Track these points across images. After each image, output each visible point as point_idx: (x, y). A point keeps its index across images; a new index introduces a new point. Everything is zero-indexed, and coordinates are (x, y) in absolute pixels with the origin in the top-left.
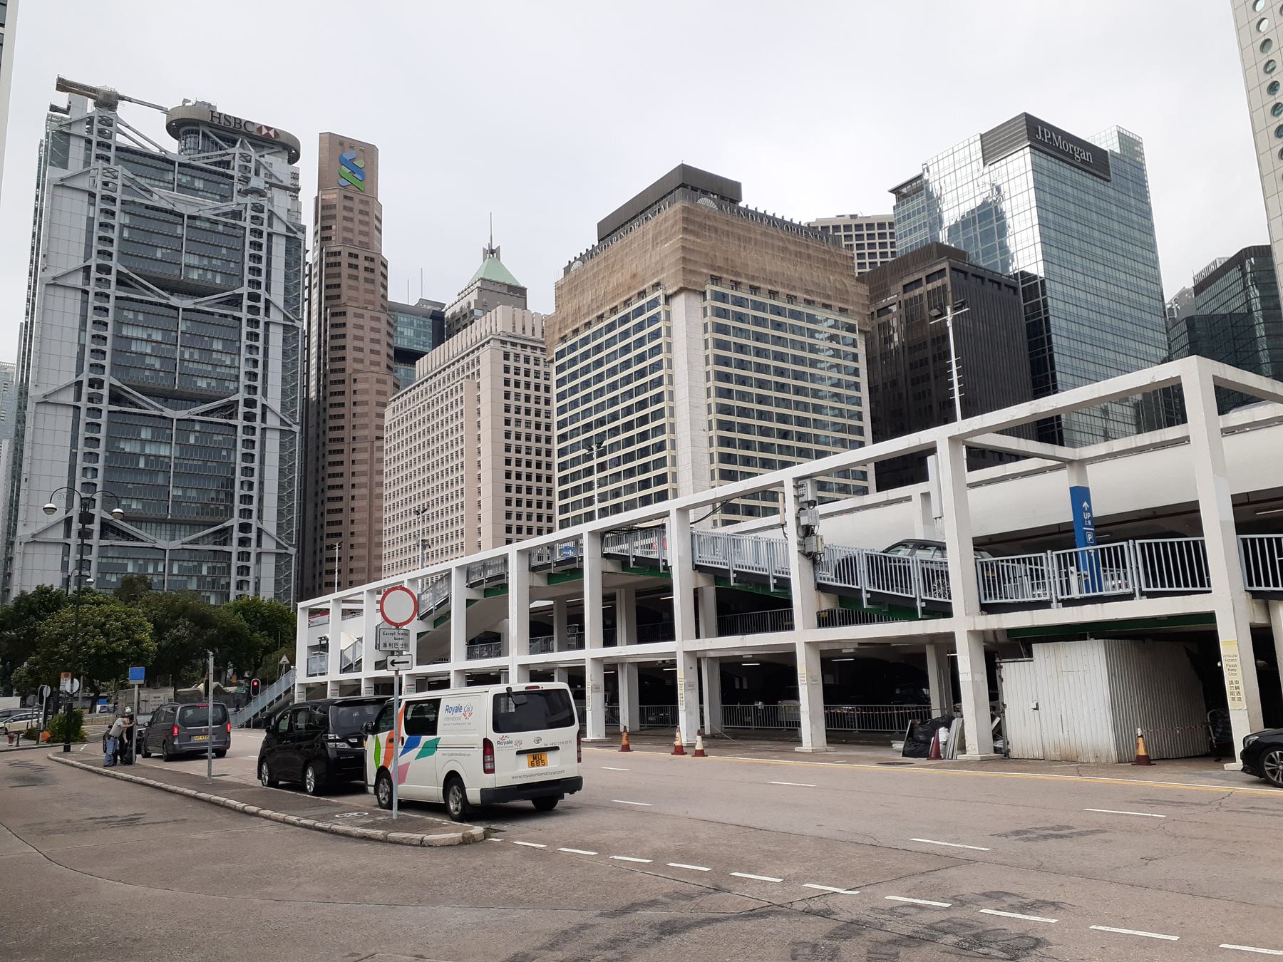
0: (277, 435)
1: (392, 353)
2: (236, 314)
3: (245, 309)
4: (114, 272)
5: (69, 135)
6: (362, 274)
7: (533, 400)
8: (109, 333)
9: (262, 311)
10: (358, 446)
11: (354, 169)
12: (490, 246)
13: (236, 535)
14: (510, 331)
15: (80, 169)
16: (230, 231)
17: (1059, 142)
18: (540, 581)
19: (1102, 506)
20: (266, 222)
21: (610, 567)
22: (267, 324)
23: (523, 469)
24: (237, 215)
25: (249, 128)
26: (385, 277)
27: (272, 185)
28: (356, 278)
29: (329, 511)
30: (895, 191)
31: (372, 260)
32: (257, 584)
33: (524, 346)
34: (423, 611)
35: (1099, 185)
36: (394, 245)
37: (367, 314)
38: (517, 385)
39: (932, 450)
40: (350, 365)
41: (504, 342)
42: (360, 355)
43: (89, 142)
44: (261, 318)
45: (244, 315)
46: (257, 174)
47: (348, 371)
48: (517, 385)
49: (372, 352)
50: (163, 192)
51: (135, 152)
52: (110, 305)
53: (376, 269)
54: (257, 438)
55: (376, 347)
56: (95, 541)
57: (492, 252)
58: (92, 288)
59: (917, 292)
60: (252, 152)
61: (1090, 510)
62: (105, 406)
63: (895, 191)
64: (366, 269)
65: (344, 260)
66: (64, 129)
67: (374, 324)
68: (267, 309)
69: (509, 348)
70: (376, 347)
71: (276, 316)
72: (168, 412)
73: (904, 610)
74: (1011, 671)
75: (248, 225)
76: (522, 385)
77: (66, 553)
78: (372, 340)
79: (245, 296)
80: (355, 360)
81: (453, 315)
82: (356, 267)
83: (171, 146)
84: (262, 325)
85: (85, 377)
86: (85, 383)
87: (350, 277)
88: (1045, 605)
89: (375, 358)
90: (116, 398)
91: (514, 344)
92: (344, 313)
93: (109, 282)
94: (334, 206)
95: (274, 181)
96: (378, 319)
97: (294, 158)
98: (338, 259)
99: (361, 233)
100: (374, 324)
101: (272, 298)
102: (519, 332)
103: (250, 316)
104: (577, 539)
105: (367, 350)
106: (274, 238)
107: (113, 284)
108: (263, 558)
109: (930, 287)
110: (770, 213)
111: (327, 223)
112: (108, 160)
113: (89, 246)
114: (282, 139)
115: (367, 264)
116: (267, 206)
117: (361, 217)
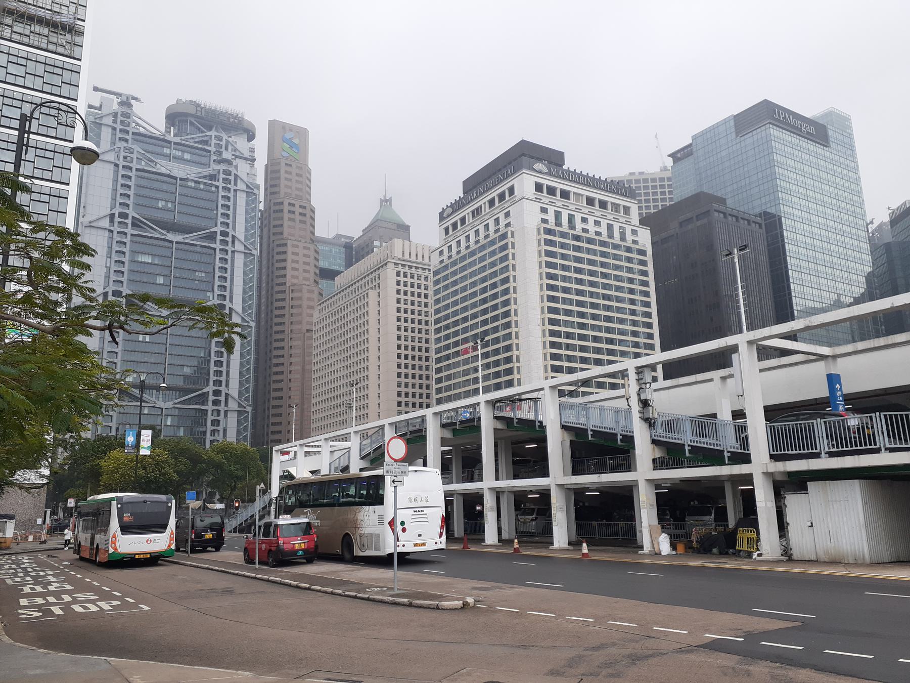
1: (318, 272)
2: (212, 245)
3: (218, 242)
4: (130, 217)
5: (101, 124)
6: (298, 217)
7: (416, 304)
8: (126, 259)
9: (230, 244)
10: (293, 336)
11: (292, 146)
12: (385, 197)
13: (211, 398)
14: (400, 256)
15: (108, 148)
16: (208, 188)
17: (791, 120)
18: (448, 434)
19: (850, 386)
20: (232, 182)
21: (499, 426)
22: (233, 252)
23: (410, 353)
24: (213, 177)
26: (314, 219)
27: (236, 157)
28: (293, 220)
29: (274, 382)
30: (672, 155)
31: (305, 208)
32: (225, 430)
33: (410, 267)
34: (364, 453)
35: (820, 150)
36: (320, 197)
37: (301, 245)
38: (405, 293)
39: (734, 349)
40: (290, 280)
41: (396, 264)
42: (296, 273)
43: (114, 129)
44: (229, 248)
45: (218, 246)
46: (226, 149)
47: (288, 285)
48: (405, 293)
49: (305, 271)
50: (163, 162)
51: (145, 136)
52: (128, 240)
53: (307, 215)
55: (307, 268)
57: (386, 201)
58: (116, 228)
59: (690, 227)
61: (841, 390)
63: (672, 155)
64: (301, 214)
65: (286, 208)
66: (98, 121)
67: (306, 252)
68: (233, 242)
69: (400, 268)
70: (307, 268)
71: (239, 247)
73: (714, 457)
74: (793, 501)
75: (221, 184)
76: (409, 294)
78: (305, 263)
79: (219, 233)
80: (293, 277)
81: (359, 246)
82: (294, 212)
84: (230, 253)
86: (110, 293)
87: (290, 219)
88: (817, 456)
89: (306, 275)
91: (403, 265)
92: (285, 245)
93: (126, 224)
94: (279, 171)
95: (237, 154)
96: (308, 249)
97: (251, 137)
98: (281, 207)
99: (297, 189)
100: (306, 252)
101: (237, 235)
102: (407, 257)
103: (221, 247)
104: (475, 406)
105: (301, 270)
106: (238, 192)
107: (130, 226)
108: (229, 414)
109: (699, 223)
110: (584, 173)
111: (273, 183)
112: (127, 141)
113: (114, 199)
114: (245, 126)
115: (301, 210)
116: (234, 171)
117: (297, 178)
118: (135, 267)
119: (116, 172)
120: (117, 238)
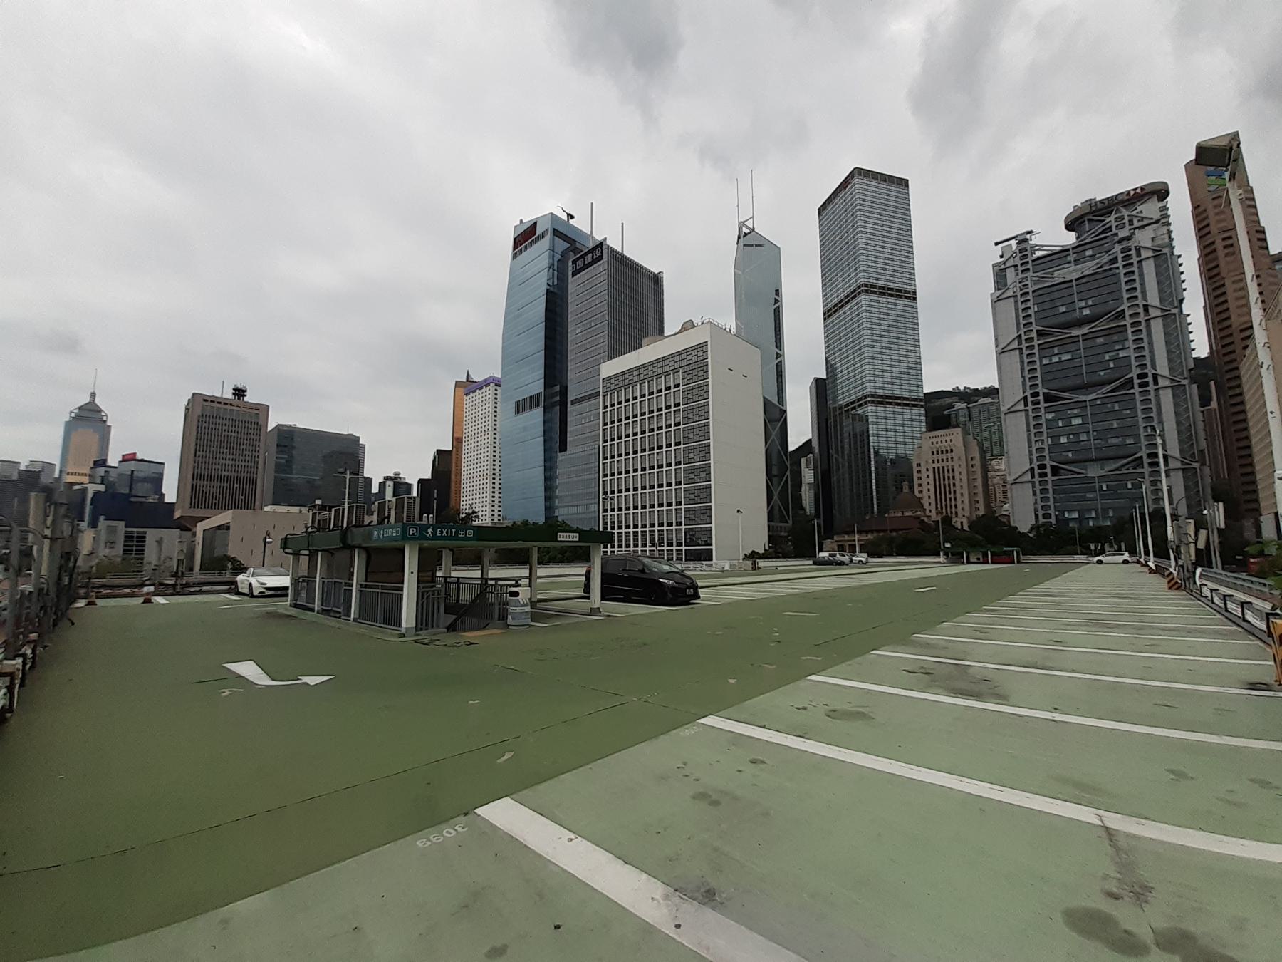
0: (1170, 390)
13: (1146, 461)
25: (1120, 198)
44: (1142, 318)
46: (1131, 222)
54: (1152, 396)
56: (1050, 478)
58: (1024, 345)
60: (1125, 213)
62: (1042, 405)
71: (1153, 313)
72: (1082, 398)
75: (1120, 264)
77: (1034, 486)
83: (1070, 238)
85: (1028, 394)
90: (1048, 398)
95: (1146, 222)
101: (1149, 302)
108: (1172, 474)
113: (1018, 324)
114: (1147, 190)
118: (1048, 369)
119: (1016, 302)
120: (1026, 352)
